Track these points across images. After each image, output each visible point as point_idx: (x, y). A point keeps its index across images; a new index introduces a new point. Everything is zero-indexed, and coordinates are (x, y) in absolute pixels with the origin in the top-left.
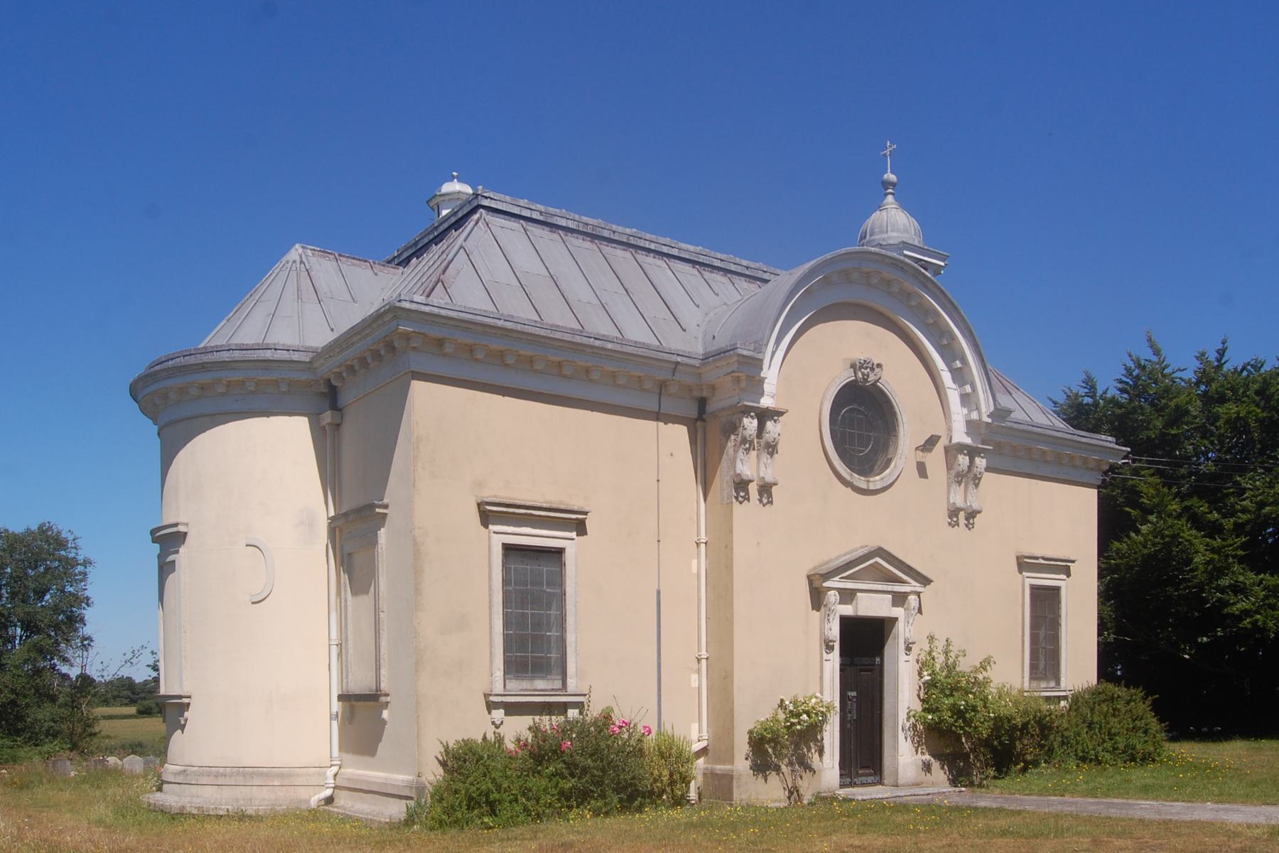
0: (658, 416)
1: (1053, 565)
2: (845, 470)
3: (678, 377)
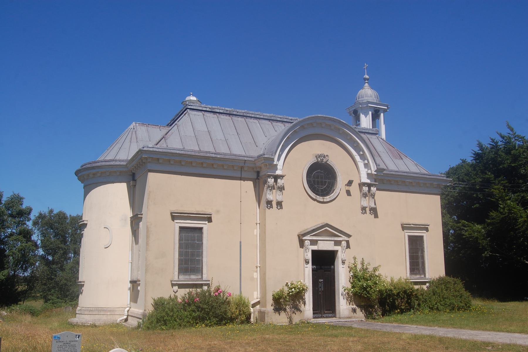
0: (241, 179)
1: (418, 227)
3: (246, 165)
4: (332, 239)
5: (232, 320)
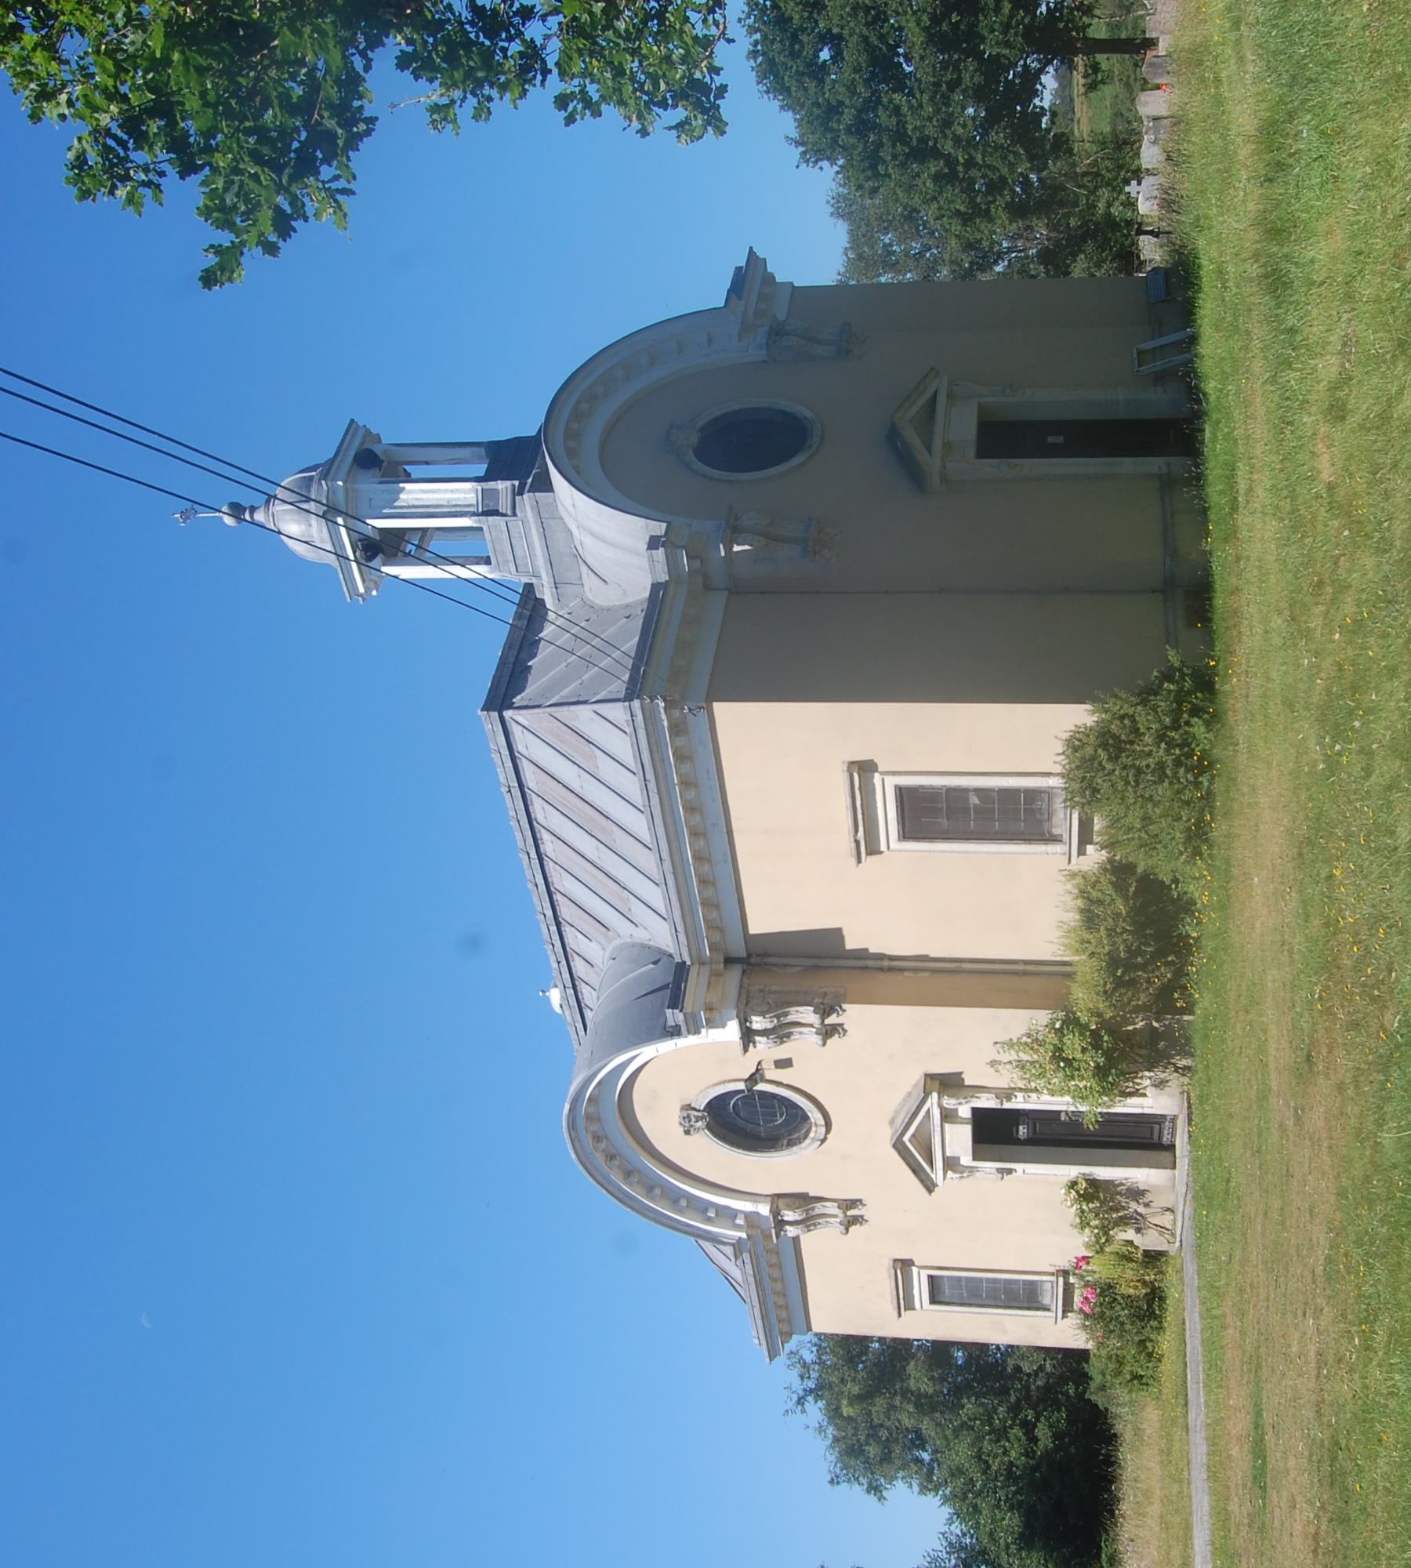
1: (863, 814)
2: (809, 1145)
4: (939, 1129)
5: (1156, 1295)
